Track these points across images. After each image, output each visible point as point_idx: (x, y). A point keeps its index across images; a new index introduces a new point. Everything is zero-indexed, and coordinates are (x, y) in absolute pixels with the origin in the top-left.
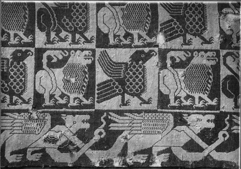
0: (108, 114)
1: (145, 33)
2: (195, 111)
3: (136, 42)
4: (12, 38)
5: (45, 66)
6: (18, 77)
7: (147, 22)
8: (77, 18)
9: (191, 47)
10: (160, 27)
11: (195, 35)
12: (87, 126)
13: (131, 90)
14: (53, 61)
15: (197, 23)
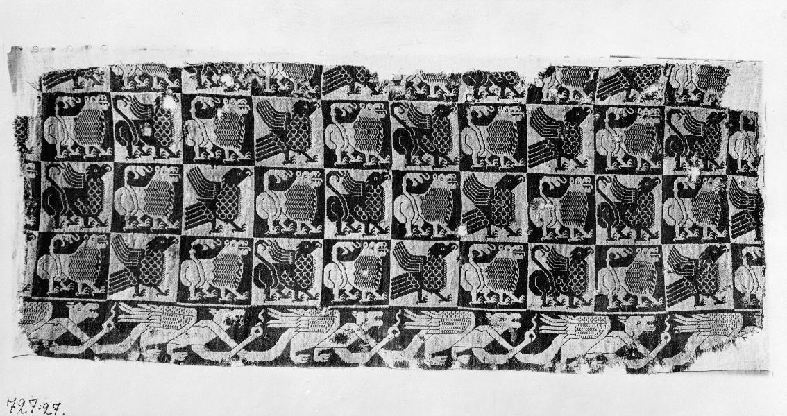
0: (403, 311)
1: (446, 224)
2: (499, 310)
3: (436, 234)
4: (299, 228)
5: (334, 259)
6: (305, 271)
7: (448, 212)
8: (372, 206)
9: (497, 240)
10: (462, 218)
11: (501, 226)
12: (380, 323)
13: (429, 286)
14: (343, 254)
15: (504, 214)
